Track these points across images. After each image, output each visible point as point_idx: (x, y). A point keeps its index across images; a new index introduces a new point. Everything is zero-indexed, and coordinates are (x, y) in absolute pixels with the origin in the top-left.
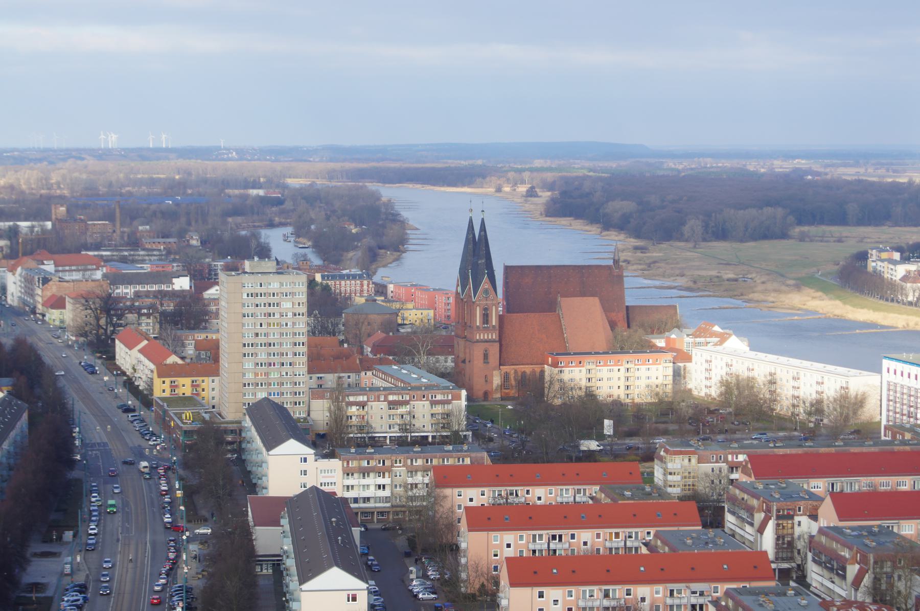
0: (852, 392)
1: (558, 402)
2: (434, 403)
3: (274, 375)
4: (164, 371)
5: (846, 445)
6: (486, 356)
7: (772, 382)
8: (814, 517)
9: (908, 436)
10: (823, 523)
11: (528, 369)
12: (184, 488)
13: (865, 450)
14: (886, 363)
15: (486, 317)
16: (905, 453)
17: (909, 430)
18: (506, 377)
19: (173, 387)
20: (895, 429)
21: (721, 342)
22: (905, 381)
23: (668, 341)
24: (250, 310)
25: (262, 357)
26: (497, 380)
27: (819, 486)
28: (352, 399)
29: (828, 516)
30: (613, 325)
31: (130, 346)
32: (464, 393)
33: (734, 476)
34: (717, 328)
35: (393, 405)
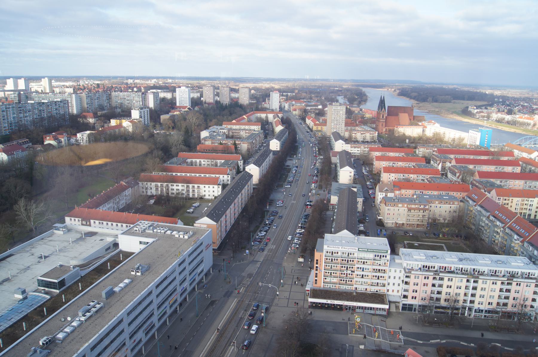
0: (462, 137)
1: (397, 135)
2: (370, 134)
3: (338, 127)
4: (315, 125)
6: (382, 125)
7: (444, 134)
8: (450, 163)
9: (473, 147)
10: (452, 164)
11: (391, 128)
12: (318, 148)
14: (470, 131)
15: (383, 117)
17: (474, 146)
18: (386, 129)
19: (317, 128)
20: (471, 145)
21: (434, 124)
23: (422, 123)
24: (334, 113)
25: (335, 123)
26: (384, 130)
27: (452, 156)
28: (353, 132)
29: (454, 163)
30: (410, 120)
31: (309, 119)
32: (377, 132)
33: (433, 153)
34: (433, 121)
35: (362, 134)
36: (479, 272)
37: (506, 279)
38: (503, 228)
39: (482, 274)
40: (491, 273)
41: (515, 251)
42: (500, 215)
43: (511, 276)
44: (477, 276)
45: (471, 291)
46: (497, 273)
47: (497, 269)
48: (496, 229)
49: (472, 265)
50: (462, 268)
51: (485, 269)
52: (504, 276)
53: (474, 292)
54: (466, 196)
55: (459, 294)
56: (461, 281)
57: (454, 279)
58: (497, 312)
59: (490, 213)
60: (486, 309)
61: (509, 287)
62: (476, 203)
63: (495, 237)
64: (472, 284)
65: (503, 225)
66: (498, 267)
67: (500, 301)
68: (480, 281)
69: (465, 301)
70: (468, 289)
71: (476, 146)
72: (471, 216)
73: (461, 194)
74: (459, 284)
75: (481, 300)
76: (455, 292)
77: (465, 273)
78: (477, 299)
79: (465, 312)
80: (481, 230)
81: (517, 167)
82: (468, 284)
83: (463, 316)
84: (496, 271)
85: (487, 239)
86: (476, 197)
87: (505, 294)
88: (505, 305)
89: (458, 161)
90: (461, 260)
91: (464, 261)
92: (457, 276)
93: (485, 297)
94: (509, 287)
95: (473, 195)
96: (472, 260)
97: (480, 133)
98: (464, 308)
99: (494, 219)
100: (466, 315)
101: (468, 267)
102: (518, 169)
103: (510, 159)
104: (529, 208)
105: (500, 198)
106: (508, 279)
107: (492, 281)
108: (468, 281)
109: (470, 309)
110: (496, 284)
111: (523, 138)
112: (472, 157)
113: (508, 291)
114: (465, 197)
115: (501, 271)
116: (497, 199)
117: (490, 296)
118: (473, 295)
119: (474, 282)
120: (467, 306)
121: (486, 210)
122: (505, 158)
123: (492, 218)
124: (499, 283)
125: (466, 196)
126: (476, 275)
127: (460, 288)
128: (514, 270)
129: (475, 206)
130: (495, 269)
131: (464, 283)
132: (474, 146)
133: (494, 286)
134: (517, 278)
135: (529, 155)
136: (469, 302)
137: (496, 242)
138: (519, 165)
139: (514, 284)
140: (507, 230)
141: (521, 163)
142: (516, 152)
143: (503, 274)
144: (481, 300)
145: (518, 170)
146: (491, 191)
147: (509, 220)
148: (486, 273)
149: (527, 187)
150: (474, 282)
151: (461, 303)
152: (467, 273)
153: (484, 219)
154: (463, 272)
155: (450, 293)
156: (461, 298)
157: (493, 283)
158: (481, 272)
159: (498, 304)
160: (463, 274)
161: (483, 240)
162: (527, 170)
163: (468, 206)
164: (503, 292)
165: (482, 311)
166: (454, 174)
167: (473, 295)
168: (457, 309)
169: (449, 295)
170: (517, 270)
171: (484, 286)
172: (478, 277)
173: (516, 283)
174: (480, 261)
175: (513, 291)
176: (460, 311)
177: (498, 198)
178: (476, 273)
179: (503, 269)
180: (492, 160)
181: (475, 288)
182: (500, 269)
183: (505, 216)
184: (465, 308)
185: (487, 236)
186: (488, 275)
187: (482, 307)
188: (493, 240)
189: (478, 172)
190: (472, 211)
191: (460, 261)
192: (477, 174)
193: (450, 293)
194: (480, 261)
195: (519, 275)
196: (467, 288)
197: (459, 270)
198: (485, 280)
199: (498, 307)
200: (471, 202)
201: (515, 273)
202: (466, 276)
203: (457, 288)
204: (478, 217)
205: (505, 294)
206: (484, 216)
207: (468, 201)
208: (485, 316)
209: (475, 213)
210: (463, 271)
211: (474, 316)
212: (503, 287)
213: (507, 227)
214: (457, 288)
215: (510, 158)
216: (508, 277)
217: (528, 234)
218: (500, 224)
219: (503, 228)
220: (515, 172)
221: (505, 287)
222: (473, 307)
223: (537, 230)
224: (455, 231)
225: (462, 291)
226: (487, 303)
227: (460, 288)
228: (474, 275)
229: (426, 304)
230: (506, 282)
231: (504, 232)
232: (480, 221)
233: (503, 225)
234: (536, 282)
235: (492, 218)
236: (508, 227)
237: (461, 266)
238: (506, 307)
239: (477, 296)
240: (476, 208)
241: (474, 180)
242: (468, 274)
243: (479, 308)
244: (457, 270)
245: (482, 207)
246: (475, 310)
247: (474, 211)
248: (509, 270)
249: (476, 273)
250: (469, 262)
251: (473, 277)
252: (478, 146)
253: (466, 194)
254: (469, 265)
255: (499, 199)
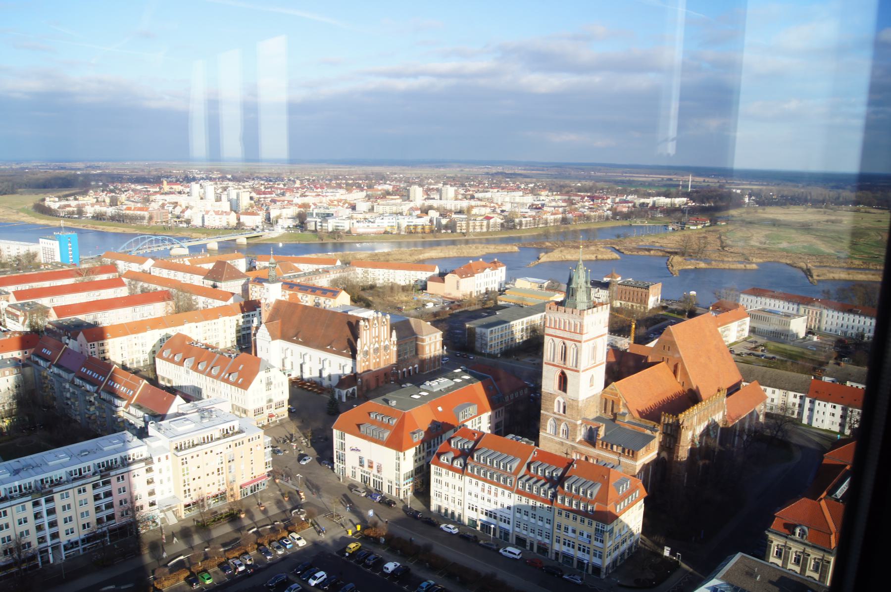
5: (24, 272)
8: (8, 301)
9: (50, 266)
13: (31, 273)
14: (41, 240)
16: (48, 273)
17: (50, 264)
20: (47, 264)
22: (49, 246)
27: (11, 289)
29: (13, 300)
36: (52, 481)
37: (99, 477)
38: (96, 392)
39: (58, 483)
40: (74, 476)
41: (122, 424)
42: (89, 373)
43: (106, 470)
44: (50, 489)
45: (46, 520)
46: (83, 473)
47: (81, 466)
48: (87, 398)
49: (37, 474)
50: (20, 486)
51: (61, 473)
52: (94, 474)
53: (52, 518)
54: (33, 354)
55: (27, 532)
56: (24, 508)
57: (8, 510)
58: (103, 535)
59: (74, 374)
60: (82, 537)
61: (107, 488)
62: (50, 363)
63: (89, 410)
64: (44, 507)
65: (96, 388)
66: (82, 462)
67: (100, 515)
68: (57, 497)
69: (42, 540)
70: (42, 517)
71: (54, 264)
72: (47, 387)
73: (26, 353)
74: (22, 516)
75: (69, 526)
76: (18, 533)
77: (27, 492)
78: (62, 528)
79: (49, 558)
80: (68, 404)
81: (121, 288)
82: (37, 509)
83: (48, 564)
84: (80, 470)
85: (78, 418)
86: (49, 353)
87: (104, 502)
88: (111, 517)
89: (19, 295)
90: (16, 472)
91: (22, 474)
92: (13, 502)
93: (74, 518)
94: (107, 488)
95: (44, 350)
96: (37, 466)
97: (57, 242)
98: (44, 551)
99: (81, 382)
100: (51, 561)
101: (31, 480)
102: (122, 290)
103: (111, 278)
104: (141, 349)
105: (94, 345)
106: (102, 477)
107: (76, 490)
108: (36, 504)
109: (55, 548)
110: (84, 490)
111: (132, 240)
112: (46, 284)
113: (108, 494)
114: (32, 356)
115: (89, 467)
116: (89, 347)
117: (82, 514)
118: (53, 524)
119: (47, 501)
120: (48, 546)
121: (69, 371)
122: (104, 277)
123: (78, 381)
124: (89, 487)
125: (33, 354)
126: (47, 490)
127: (26, 521)
128: (109, 458)
129: (50, 367)
130: (77, 467)
131: (30, 511)
132: (51, 264)
133: (83, 496)
134: (117, 468)
135: (140, 266)
136: (48, 538)
137: (92, 418)
138: (123, 284)
139: (114, 480)
140: (104, 395)
141: (124, 279)
142: (122, 266)
143: (92, 470)
144: (69, 526)
145: (122, 292)
146: (78, 334)
147: (103, 378)
148: (64, 478)
149: (138, 316)
150: (47, 501)
151: (35, 544)
152: (31, 491)
153: (67, 386)
154: (23, 492)
155: (9, 537)
156: (33, 538)
157: (80, 492)
158: (56, 480)
159: (99, 521)
160: (22, 495)
161: (76, 421)
162: (139, 290)
163: (39, 371)
164: (101, 499)
165: (76, 542)
166: (15, 317)
167: (53, 524)
168: (33, 557)
169: (9, 540)
170: (113, 457)
171: (66, 502)
172: (51, 492)
173: (116, 477)
174: (50, 463)
175: (115, 492)
176: (39, 559)
177: (91, 345)
178: (47, 486)
179: (90, 463)
180: (82, 283)
181: (51, 512)
182: (86, 465)
183: (97, 373)
184: (47, 551)
185: (78, 413)
186: (68, 482)
187: (74, 537)
188: (87, 416)
189: (54, 308)
190: (46, 378)
191: (14, 475)
192: (52, 312)
193: (9, 537)
194: (50, 463)
195: (118, 463)
196: (37, 516)
197: (16, 491)
198: (64, 492)
199: (100, 526)
200: (42, 363)
201: (112, 463)
202: (29, 498)
203: (20, 523)
204: (56, 386)
205: (104, 502)
206: (66, 381)
207: (37, 363)
208: (84, 549)
209: (51, 381)
210: (24, 491)
211: (66, 557)
212: (97, 491)
213: (102, 390)
214: (20, 523)
215: (111, 276)
216: (101, 471)
217: (132, 392)
218: (91, 387)
219: (96, 392)
220: (119, 296)
221: (101, 491)
222: (60, 542)
223: (142, 382)
224: (24, 420)
225: (31, 524)
226: (81, 527)
227: (26, 521)
228: (43, 491)
229: (8, 562)
230: (101, 481)
231: (99, 398)
232: (62, 392)
233: (96, 388)
234: (146, 465)
235: (78, 380)
236: (103, 390)
237: (17, 484)
238: (113, 521)
239: (61, 522)
240: (51, 370)
241: (49, 323)
242: (30, 494)
243: (69, 541)
244: (11, 492)
245: (58, 366)
246: (65, 546)
247: (49, 377)
248: (104, 459)
249: (47, 486)
250: (30, 471)
251: (42, 495)
252: (57, 263)
253: (32, 350)
254: (32, 476)
255: (93, 346)
